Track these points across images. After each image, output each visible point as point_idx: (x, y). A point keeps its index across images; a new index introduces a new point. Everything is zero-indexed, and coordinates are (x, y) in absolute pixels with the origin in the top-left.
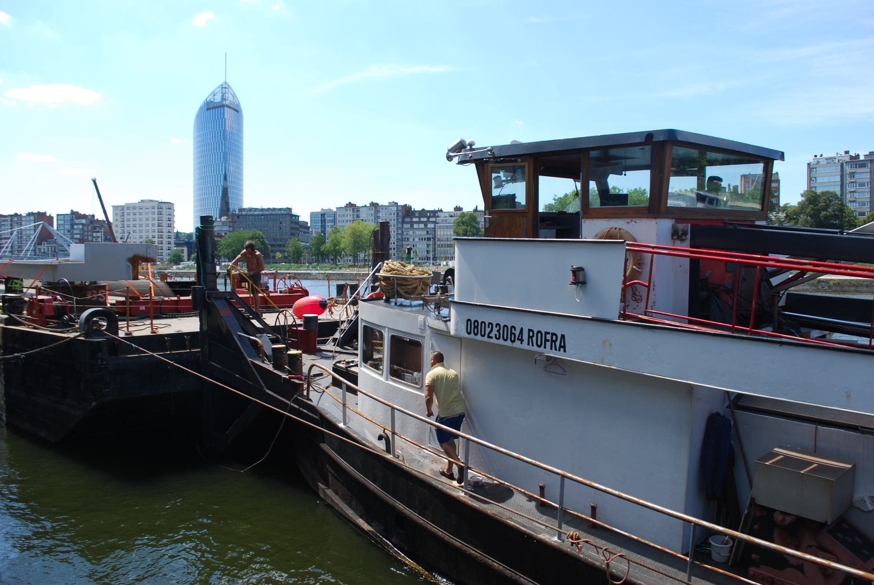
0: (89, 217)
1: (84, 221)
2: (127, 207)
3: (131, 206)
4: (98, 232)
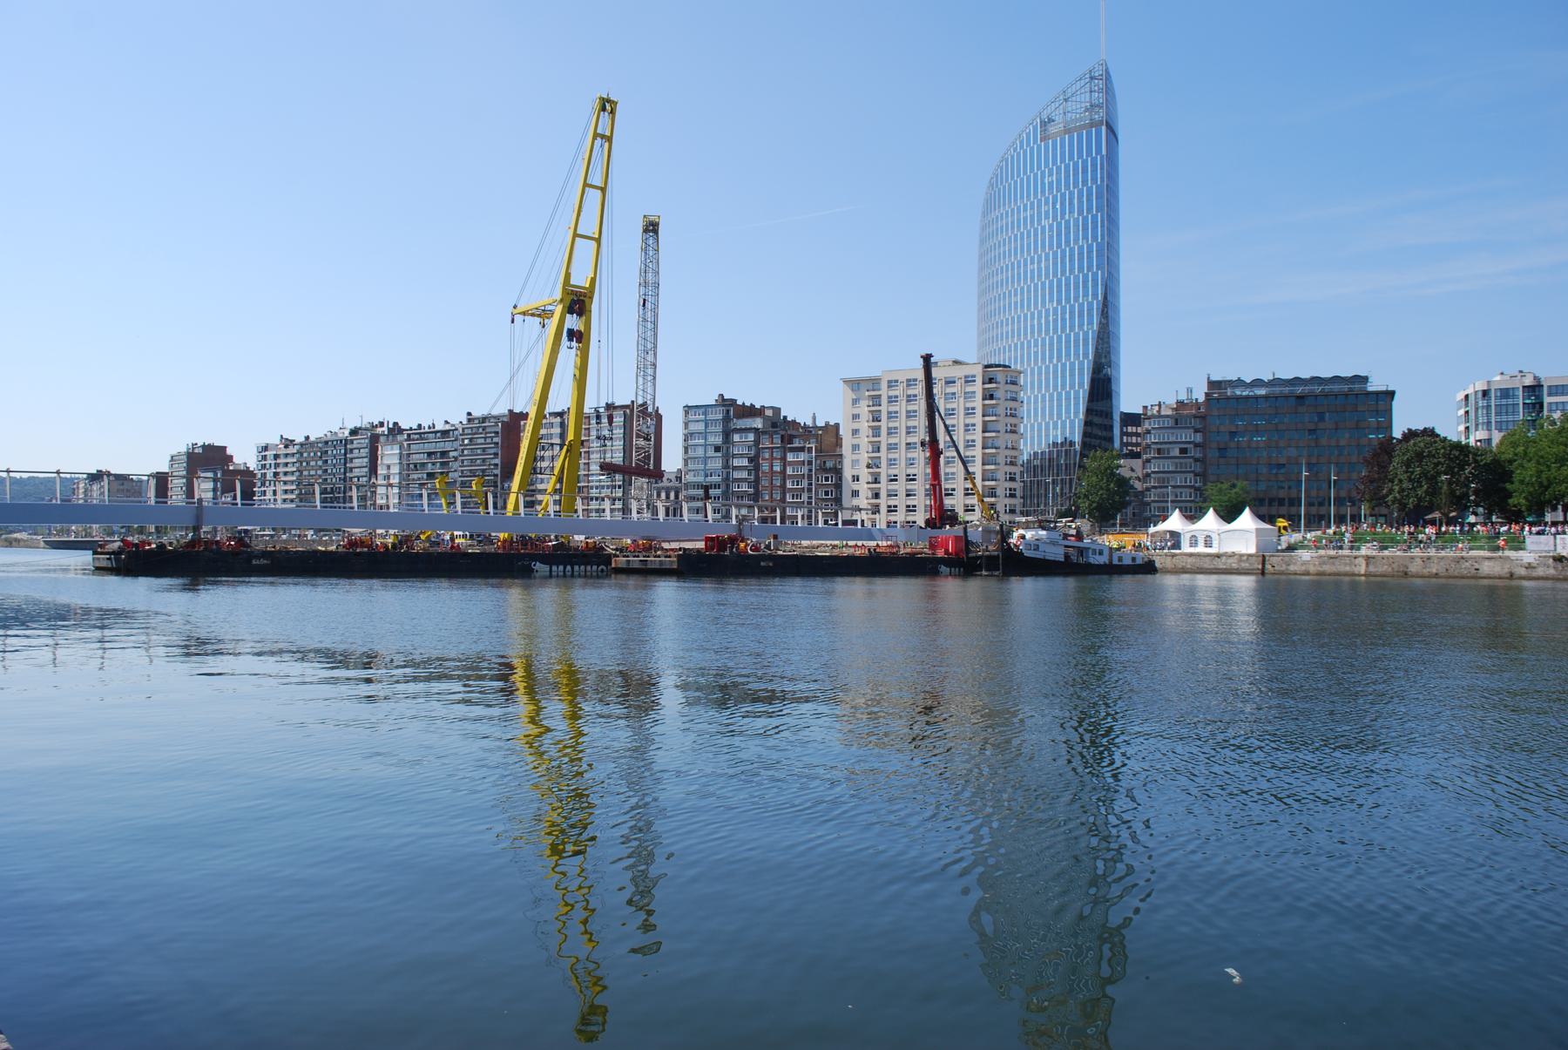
0: (769, 413)
1: (758, 423)
2: (889, 382)
3: (902, 378)
4: (802, 449)
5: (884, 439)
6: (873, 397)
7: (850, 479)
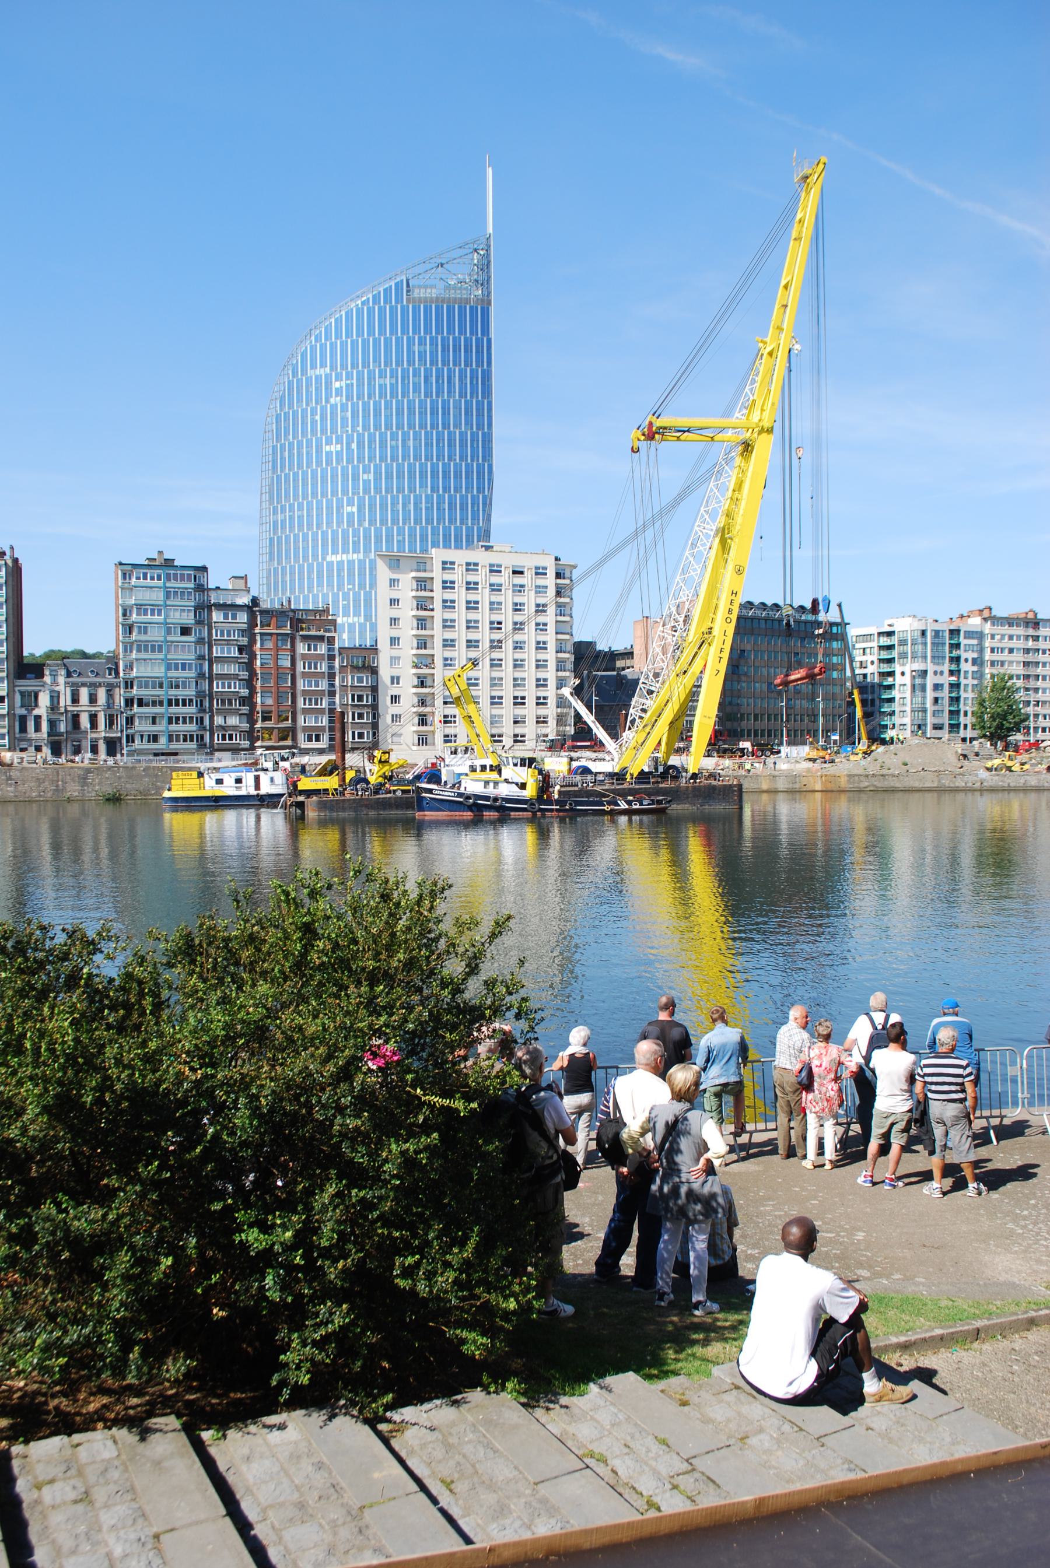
2: (444, 563)
5: (438, 632)
6: (418, 580)
7: (388, 681)
